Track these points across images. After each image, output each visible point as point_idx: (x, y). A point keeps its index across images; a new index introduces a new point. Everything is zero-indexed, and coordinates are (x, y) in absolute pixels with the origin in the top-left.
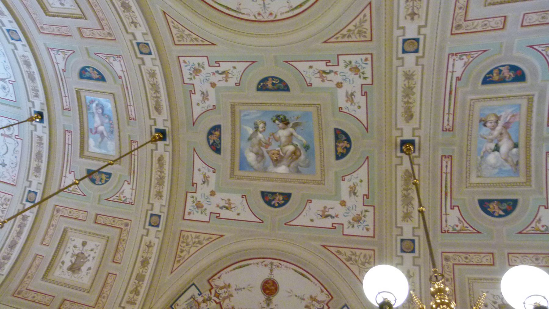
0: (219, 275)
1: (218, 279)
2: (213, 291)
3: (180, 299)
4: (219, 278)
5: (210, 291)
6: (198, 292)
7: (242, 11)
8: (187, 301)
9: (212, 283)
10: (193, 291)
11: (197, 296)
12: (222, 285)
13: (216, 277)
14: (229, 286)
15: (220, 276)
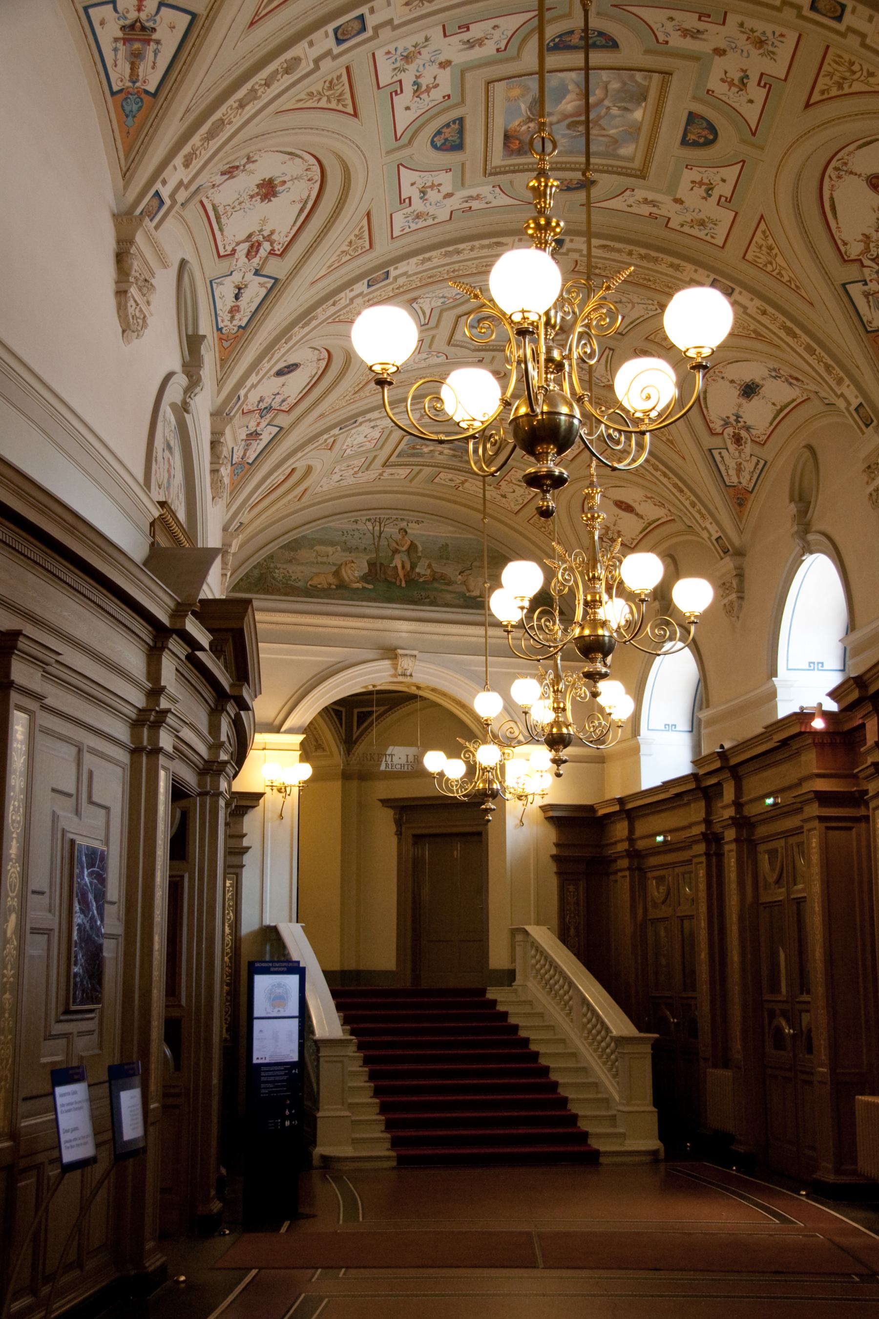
0: (839, 242)
1: (848, 247)
2: (867, 262)
3: (861, 314)
4: (845, 244)
5: (863, 266)
6: (860, 284)
7: (305, 197)
8: (870, 307)
9: (853, 257)
10: (855, 290)
11: (866, 288)
12: (861, 247)
13: (843, 249)
14: (867, 236)
15: (843, 241)
